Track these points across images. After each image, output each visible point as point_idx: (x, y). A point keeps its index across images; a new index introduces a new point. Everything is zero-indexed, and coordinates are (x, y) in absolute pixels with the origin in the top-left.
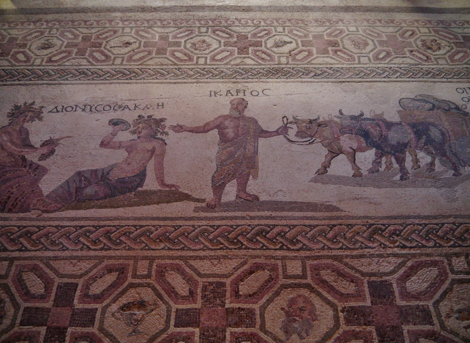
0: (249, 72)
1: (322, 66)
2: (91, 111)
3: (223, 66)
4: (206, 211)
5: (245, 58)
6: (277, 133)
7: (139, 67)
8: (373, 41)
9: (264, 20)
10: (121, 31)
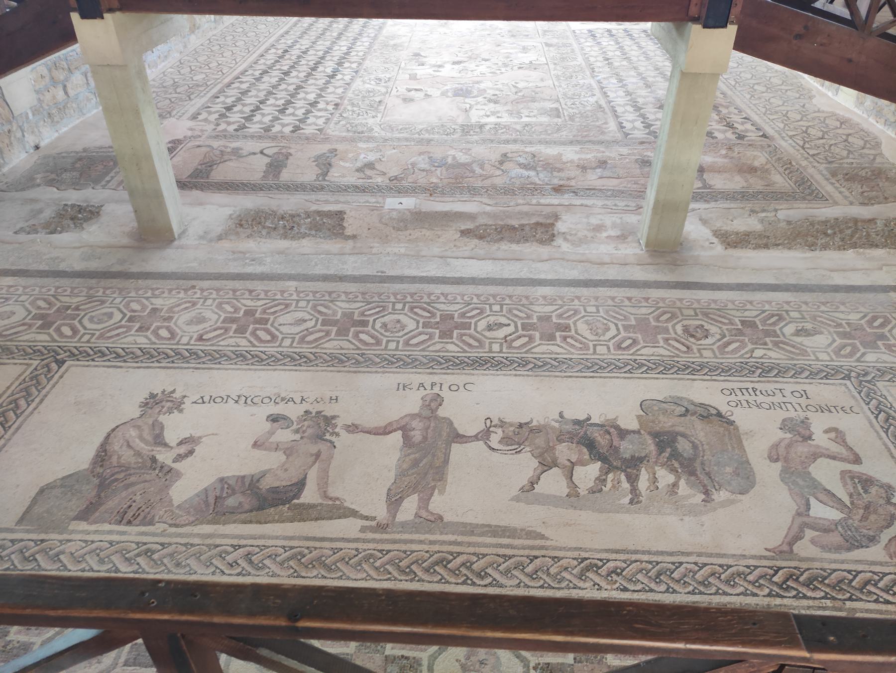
0: (450, 360)
1: (544, 356)
3: (418, 353)
4: (375, 532)
5: (447, 343)
6: (476, 438)
7: (313, 350)
8: (616, 325)
9: (478, 296)
10: (294, 305)
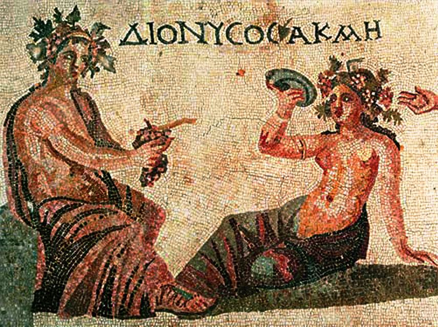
2: (218, 43)
